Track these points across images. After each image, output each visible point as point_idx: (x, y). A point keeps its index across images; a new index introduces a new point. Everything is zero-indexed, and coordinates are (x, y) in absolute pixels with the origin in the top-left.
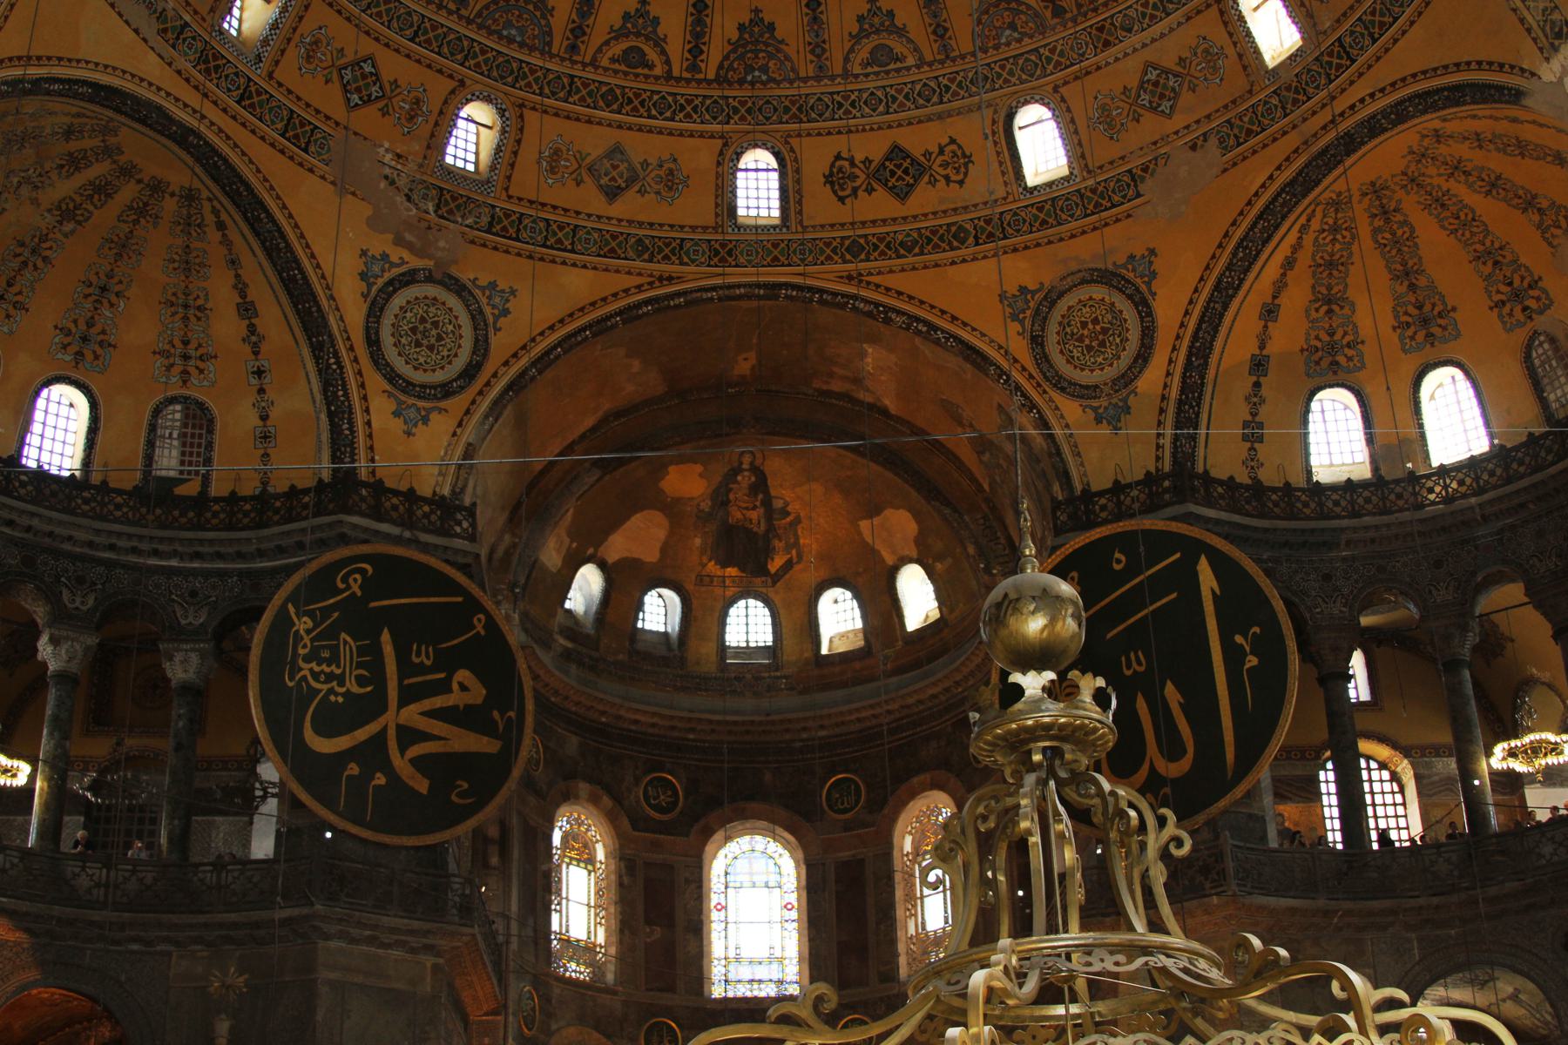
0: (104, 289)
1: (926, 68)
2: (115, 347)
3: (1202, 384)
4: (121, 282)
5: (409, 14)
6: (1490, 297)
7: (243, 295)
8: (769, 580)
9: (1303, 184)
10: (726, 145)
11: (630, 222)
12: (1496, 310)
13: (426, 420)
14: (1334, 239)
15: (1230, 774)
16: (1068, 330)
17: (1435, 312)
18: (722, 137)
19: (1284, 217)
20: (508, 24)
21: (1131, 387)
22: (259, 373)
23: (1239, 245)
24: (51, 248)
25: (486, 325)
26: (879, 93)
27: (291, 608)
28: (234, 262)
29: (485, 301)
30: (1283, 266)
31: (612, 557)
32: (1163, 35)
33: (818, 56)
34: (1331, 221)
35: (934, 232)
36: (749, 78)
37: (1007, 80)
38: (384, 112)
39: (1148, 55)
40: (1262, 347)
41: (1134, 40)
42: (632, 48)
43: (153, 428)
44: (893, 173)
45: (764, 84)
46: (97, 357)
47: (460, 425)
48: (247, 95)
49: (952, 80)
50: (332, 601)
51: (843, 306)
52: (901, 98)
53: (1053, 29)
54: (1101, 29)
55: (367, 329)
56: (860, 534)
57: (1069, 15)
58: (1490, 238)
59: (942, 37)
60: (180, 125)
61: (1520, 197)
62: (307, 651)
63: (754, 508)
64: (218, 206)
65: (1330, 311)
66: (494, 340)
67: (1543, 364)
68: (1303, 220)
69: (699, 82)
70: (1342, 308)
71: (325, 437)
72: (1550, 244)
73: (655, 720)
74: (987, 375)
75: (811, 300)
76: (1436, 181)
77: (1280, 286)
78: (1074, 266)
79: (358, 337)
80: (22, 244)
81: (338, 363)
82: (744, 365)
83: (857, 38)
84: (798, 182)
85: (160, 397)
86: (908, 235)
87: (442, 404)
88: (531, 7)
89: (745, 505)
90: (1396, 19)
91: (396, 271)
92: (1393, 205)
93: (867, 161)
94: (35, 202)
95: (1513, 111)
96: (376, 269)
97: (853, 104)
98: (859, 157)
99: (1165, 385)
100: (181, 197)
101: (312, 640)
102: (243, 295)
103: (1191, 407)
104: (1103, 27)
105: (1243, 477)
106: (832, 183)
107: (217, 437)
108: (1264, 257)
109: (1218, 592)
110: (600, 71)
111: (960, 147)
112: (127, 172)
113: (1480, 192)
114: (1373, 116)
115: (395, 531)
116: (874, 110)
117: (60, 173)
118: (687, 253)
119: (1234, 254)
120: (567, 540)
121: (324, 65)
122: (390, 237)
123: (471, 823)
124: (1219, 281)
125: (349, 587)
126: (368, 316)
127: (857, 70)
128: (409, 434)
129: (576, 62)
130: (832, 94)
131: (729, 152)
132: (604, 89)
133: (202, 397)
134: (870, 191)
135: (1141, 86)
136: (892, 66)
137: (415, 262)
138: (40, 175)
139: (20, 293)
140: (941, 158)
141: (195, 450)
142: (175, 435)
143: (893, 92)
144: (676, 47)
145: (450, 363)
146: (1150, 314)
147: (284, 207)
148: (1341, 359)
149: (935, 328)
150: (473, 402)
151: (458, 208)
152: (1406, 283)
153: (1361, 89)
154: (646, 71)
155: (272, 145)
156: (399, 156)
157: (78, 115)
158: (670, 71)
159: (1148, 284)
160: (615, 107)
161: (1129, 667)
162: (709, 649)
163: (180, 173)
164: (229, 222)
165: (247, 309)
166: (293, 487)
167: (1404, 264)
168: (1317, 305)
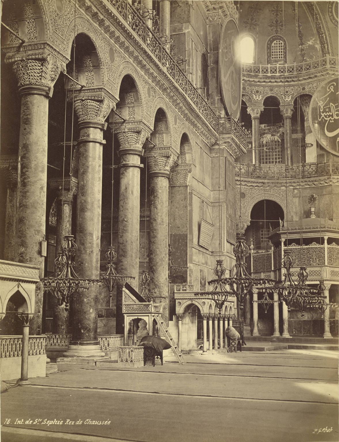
101: (323, 107)
125: (331, 90)
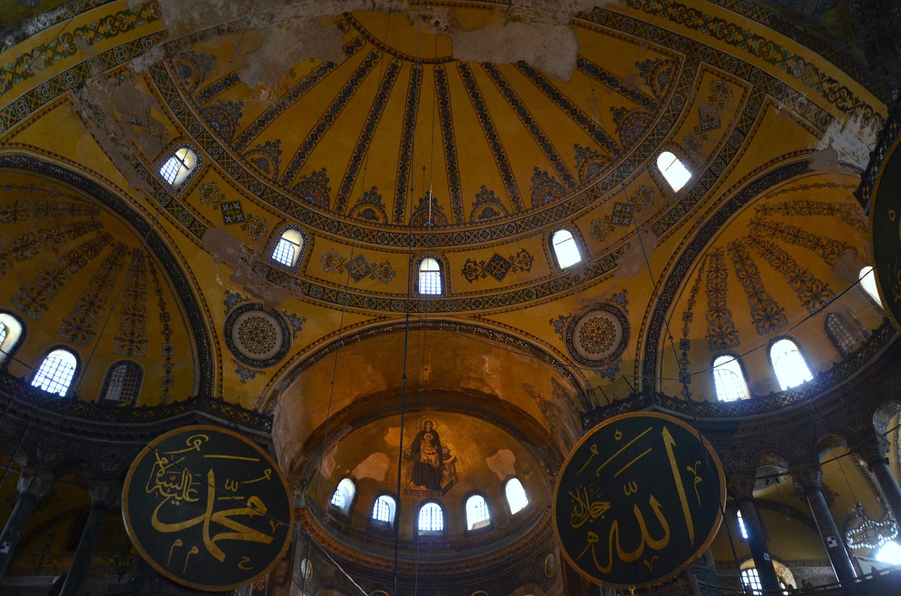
0: (92, 303)
1: (510, 217)
3: (656, 352)
5: (259, 184)
7: (163, 309)
8: (441, 493)
9: (699, 243)
11: (366, 291)
13: (253, 377)
14: (717, 276)
16: (585, 335)
19: (690, 263)
21: (619, 358)
22: (168, 350)
23: (669, 279)
24: (64, 278)
25: (289, 334)
26: (487, 231)
28: (159, 292)
31: (359, 477)
33: (458, 214)
34: (714, 266)
36: (425, 225)
37: (548, 220)
39: (617, 199)
40: (685, 335)
41: (609, 193)
42: (368, 209)
43: (109, 376)
44: (495, 268)
46: (84, 338)
47: (271, 380)
48: (170, 205)
49: (522, 222)
50: (182, 451)
51: (471, 332)
52: (498, 232)
53: (570, 193)
54: (592, 191)
55: (226, 328)
56: (486, 465)
57: (576, 186)
59: (517, 202)
60: (131, 210)
62: (161, 475)
63: (433, 454)
65: (718, 316)
66: (292, 342)
68: (700, 265)
70: (724, 314)
71: (198, 380)
73: (379, 562)
74: (545, 361)
75: (456, 329)
76: (768, 238)
77: (691, 303)
78: (586, 303)
79: (220, 332)
81: (208, 343)
82: (426, 375)
83: (476, 205)
84: (449, 273)
86: (503, 296)
87: (263, 370)
88: (319, 187)
89: (428, 452)
90: (737, 150)
91: (243, 303)
93: (482, 263)
94: (55, 250)
96: (233, 300)
98: (478, 261)
99: (637, 355)
101: (166, 470)
102: (163, 309)
104: (593, 189)
105: (681, 397)
106: (465, 274)
108: (682, 285)
109: (675, 445)
110: (353, 220)
111: (527, 253)
114: (731, 200)
115: (226, 422)
116: (485, 239)
117: (69, 235)
118: (394, 306)
119: (667, 285)
120: (335, 464)
121: (214, 201)
122: (242, 286)
125: (193, 445)
126: (227, 323)
127: (477, 220)
128: (243, 382)
129: (341, 215)
130: (465, 232)
131: (416, 260)
133: (138, 362)
134: (484, 276)
136: (493, 218)
137: (255, 301)
138: (58, 235)
139: (44, 299)
140: (518, 259)
141: (130, 388)
142: (121, 380)
143: (494, 230)
144: (390, 210)
145: (269, 350)
146: (626, 321)
147: (186, 262)
148: (727, 341)
150: (280, 371)
153: (724, 189)
154: (375, 221)
155: (182, 232)
156: (250, 250)
157: (77, 198)
158: (386, 222)
159: (624, 307)
160: (360, 238)
161: (628, 490)
162: (409, 528)
163: (135, 242)
164: (157, 270)
165: (165, 317)
166: (175, 401)
168: (712, 313)
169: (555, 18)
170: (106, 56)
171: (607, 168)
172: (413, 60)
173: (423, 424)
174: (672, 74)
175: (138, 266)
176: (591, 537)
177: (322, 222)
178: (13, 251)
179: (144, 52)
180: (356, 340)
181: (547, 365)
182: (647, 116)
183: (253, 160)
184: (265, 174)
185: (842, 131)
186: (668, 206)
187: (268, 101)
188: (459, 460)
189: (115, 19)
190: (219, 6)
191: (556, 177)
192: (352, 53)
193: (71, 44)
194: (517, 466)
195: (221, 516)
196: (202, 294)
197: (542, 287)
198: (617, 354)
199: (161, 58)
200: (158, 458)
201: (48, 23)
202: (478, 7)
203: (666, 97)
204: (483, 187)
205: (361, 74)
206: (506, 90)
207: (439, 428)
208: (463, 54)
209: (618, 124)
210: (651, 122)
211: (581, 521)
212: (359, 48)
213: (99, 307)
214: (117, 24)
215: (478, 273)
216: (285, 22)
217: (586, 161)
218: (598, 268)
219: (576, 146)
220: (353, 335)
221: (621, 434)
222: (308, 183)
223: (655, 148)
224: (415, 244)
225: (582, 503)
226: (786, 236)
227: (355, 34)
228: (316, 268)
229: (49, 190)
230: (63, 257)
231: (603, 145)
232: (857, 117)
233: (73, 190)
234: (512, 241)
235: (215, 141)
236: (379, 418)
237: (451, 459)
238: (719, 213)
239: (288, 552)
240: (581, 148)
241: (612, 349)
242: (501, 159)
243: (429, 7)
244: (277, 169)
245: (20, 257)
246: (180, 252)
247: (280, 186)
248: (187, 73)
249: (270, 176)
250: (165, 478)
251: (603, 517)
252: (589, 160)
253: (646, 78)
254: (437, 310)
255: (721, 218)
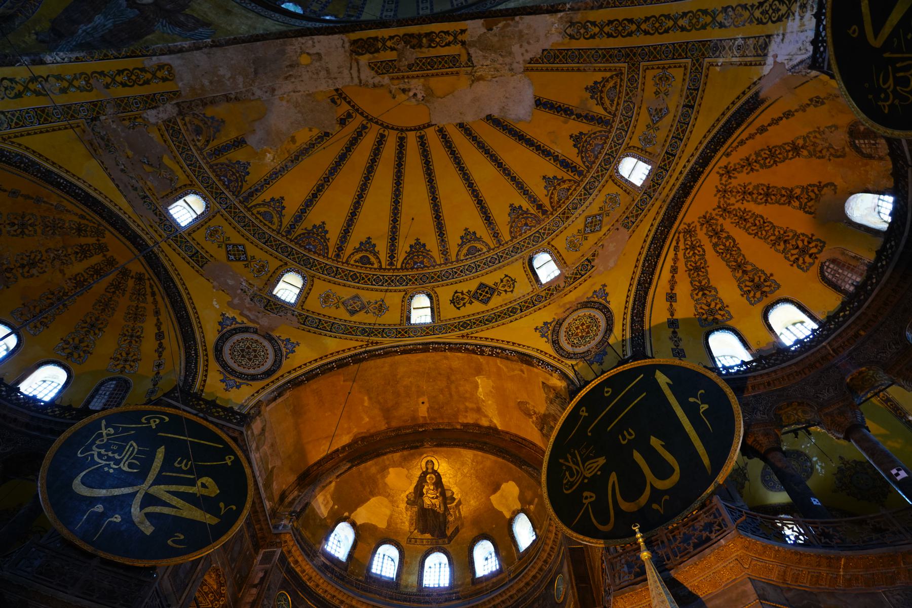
0: (93, 326)
2: (91, 354)
4: (102, 323)
5: (264, 233)
6: (789, 260)
7: (159, 329)
8: (446, 540)
9: (669, 220)
10: (406, 294)
11: (360, 323)
12: (795, 265)
13: (238, 387)
14: (694, 253)
15: (710, 472)
17: (762, 280)
18: (404, 291)
19: (664, 241)
20: (309, 244)
27: (104, 422)
29: (283, 346)
30: (671, 272)
32: (590, 203)
33: (445, 255)
34: (689, 243)
35: (501, 313)
37: (527, 247)
38: (246, 266)
39: (586, 213)
40: (672, 315)
41: (579, 211)
43: (97, 390)
44: (481, 294)
45: (422, 268)
47: (257, 392)
49: (503, 253)
51: (459, 350)
53: (544, 220)
54: (564, 214)
55: (217, 344)
56: (491, 504)
57: (549, 213)
58: (777, 230)
59: (497, 237)
60: (133, 231)
61: (784, 196)
63: (437, 497)
64: (153, 283)
65: (704, 294)
66: (284, 362)
67: (834, 276)
68: (674, 243)
69: (394, 270)
70: (710, 292)
72: (810, 213)
74: (533, 366)
76: (737, 206)
77: (673, 283)
78: (568, 306)
79: (210, 346)
80: (53, 294)
83: (460, 246)
84: (439, 304)
85: (107, 378)
87: (250, 383)
89: (431, 496)
91: (238, 325)
92: (719, 228)
93: (469, 292)
94: (61, 271)
95: (762, 118)
97: (461, 272)
98: (465, 291)
99: (623, 335)
100: (136, 279)
101: (108, 439)
102: (159, 329)
103: (638, 339)
106: (454, 303)
107: (128, 395)
109: (671, 383)
112: (102, 248)
113: (762, 203)
115: (195, 412)
120: (331, 503)
122: (239, 312)
123: (178, 560)
124: (639, 281)
126: (219, 339)
127: (462, 258)
128: (226, 390)
129: (338, 262)
132: (352, 273)
133: (127, 377)
134: (471, 303)
135: (586, 226)
138: (65, 256)
142: (107, 394)
144: (383, 256)
146: (609, 311)
149: (505, 350)
150: (268, 385)
151: (276, 308)
152: (740, 271)
153: (683, 162)
154: (370, 266)
155: (184, 259)
156: (250, 284)
157: (82, 217)
158: (381, 266)
159: (605, 300)
162: (412, 579)
165: (160, 336)
167: (736, 261)
168: (696, 292)
169: (511, 70)
170: (122, 101)
171: (575, 190)
172: (397, 129)
173: (423, 464)
174: (618, 87)
175: (139, 290)
176: (586, 498)
177: (321, 268)
178: (19, 267)
179: (158, 107)
180: (348, 364)
181: (535, 369)
182: (603, 133)
183: (258, 213)
184: (269, 225)
185: (783, 40)
186: (633, 200)
187: (272, 163)
188: (463, 502)
189: (132, 73)
190: (227, 77)
191: (530, 209)
192: (345, 124)
193: (87, 82)
194: (522, 498)
195: (160, 491)
196: (196, 313)
197: (525, 303)
198: (604, 341)
199: (175, 115)
200: (103, 427)
201: (66, 59)
202: (447, 74)
203: (617, 109)
204: (466, 229)
205: (354, 142)
206: (479, 143)
207: (440, 467)
208: (440, 120)
209: (578, 148)
210: (607, 137)
211: (573, 486)
212: (350, 120)
213: (100, 329)
214: (134, 77)
215: (466, 300)
216: (285, 96)
217: (555, 189)
218: (576, 274)
219: (544, 177)
220: (345, 358)
221: (610, 390)
222: (309, 233)
223: (615, 158)
224: (407, 283)
225: (574, 467)
226: (757, 198)
227: (345, 108)
228: (314, 304)
229: (55, 204)
230: (70, 279)
231: (568, 171)
232: (793, 14)
233: (78, 207)
234: (495, 270)
235: (223, 193)
236: (378, 455)
237: (455, 503)
238: (683, 184)
239: (261, 578)
240: (549, 178)
241: (598, 339)
242: (481, 204)
243: (406, 80)
244: (281, 222)
245: (26, 274)
246: (179, 274)
247: (283, 236)
248: (198, 131)
249: (274, 227)
250: (106, 446)
251: (599, 473)
252: (558, 187)
253: (596, 99)
254: (427, 334)
255: (686, 190)
